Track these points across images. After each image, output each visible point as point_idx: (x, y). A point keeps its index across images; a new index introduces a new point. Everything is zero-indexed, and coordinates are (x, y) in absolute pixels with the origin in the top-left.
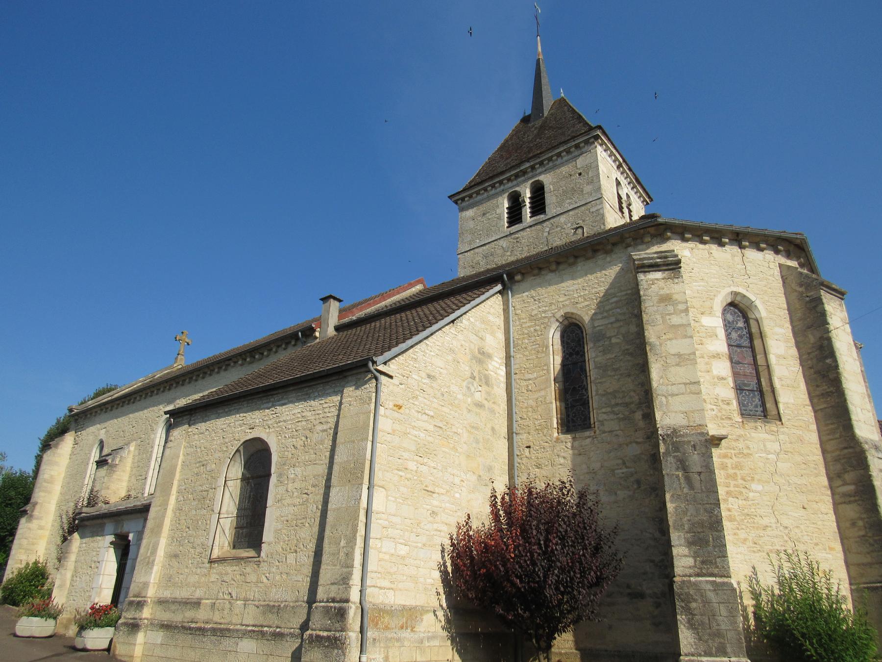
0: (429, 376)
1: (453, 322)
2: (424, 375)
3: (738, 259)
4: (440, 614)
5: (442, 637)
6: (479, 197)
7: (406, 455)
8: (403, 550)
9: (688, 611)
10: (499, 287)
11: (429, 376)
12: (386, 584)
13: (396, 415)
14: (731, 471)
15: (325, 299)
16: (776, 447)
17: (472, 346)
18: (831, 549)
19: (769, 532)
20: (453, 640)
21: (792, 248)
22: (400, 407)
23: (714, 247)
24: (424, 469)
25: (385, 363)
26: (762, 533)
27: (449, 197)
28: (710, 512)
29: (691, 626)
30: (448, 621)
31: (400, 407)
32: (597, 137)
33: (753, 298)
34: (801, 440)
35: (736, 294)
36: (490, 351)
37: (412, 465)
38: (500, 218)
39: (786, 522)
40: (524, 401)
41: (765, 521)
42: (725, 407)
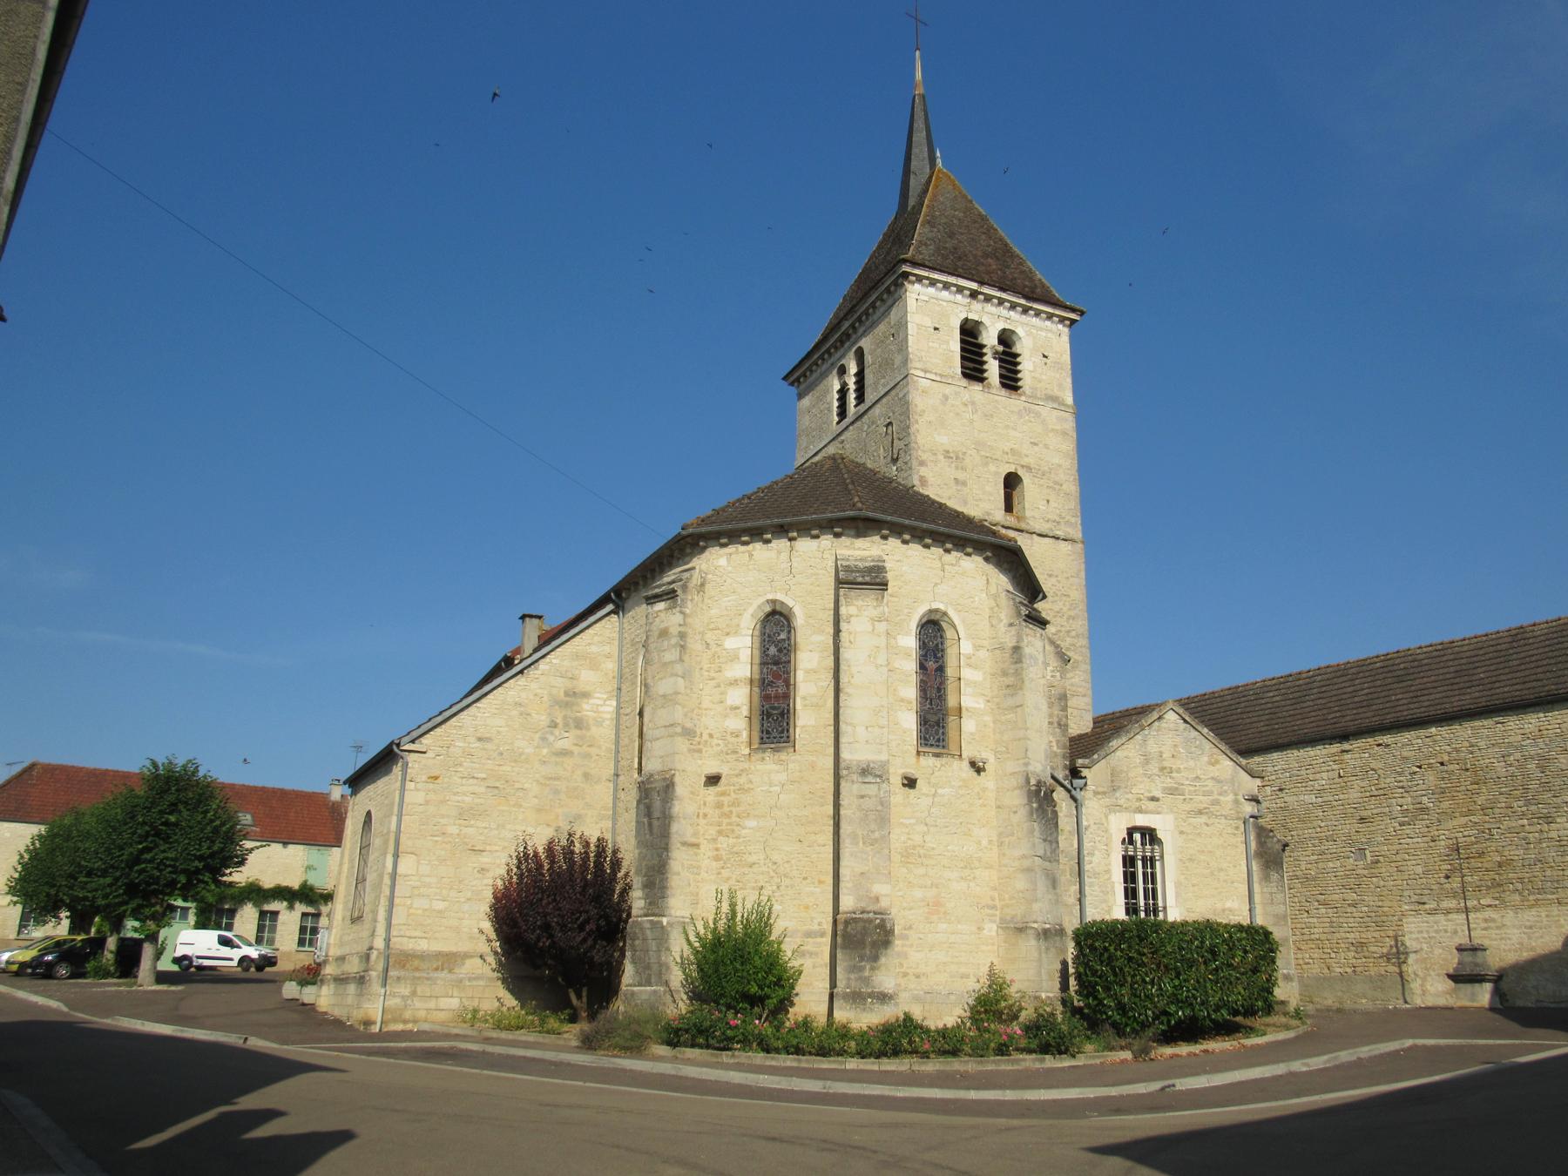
0: (480, 739)
1: (521, 672)
2: (472, 739)
3: (784, 556)
4: (491, 959)
5: (490, 979)
6: (815, 375)
7: (443, 821)
8: (440, 905)
9: (633, 946)
10: (610, 607)
11: (480, 739)
12: (417, 934)
13: (431, 786)
14: (726, 809)
15: (523, 617)
16: (783, 777)
17: (555, 691)
18: (820, 882)
19: (755, 869)
20: (504, 981)
21: (861, 524)
22: (436, 778)
23: (758, 546)
24: (470, 831)
25: (413, 741)
26: (746, 870)
27: (785, 378)
28: (660, 856)
29: (634, 962)
30: (500, 963)
31: (436, 778)
32: (906, 275)
33: (790, 603)
34: (813, 766)
35: (774, 602)
36: (588, 688)
37: (453, 830)
38: (830, 410)
39: (776, 857)
40: (624, 741)
41: (752, 859)
42: (733, 740)
